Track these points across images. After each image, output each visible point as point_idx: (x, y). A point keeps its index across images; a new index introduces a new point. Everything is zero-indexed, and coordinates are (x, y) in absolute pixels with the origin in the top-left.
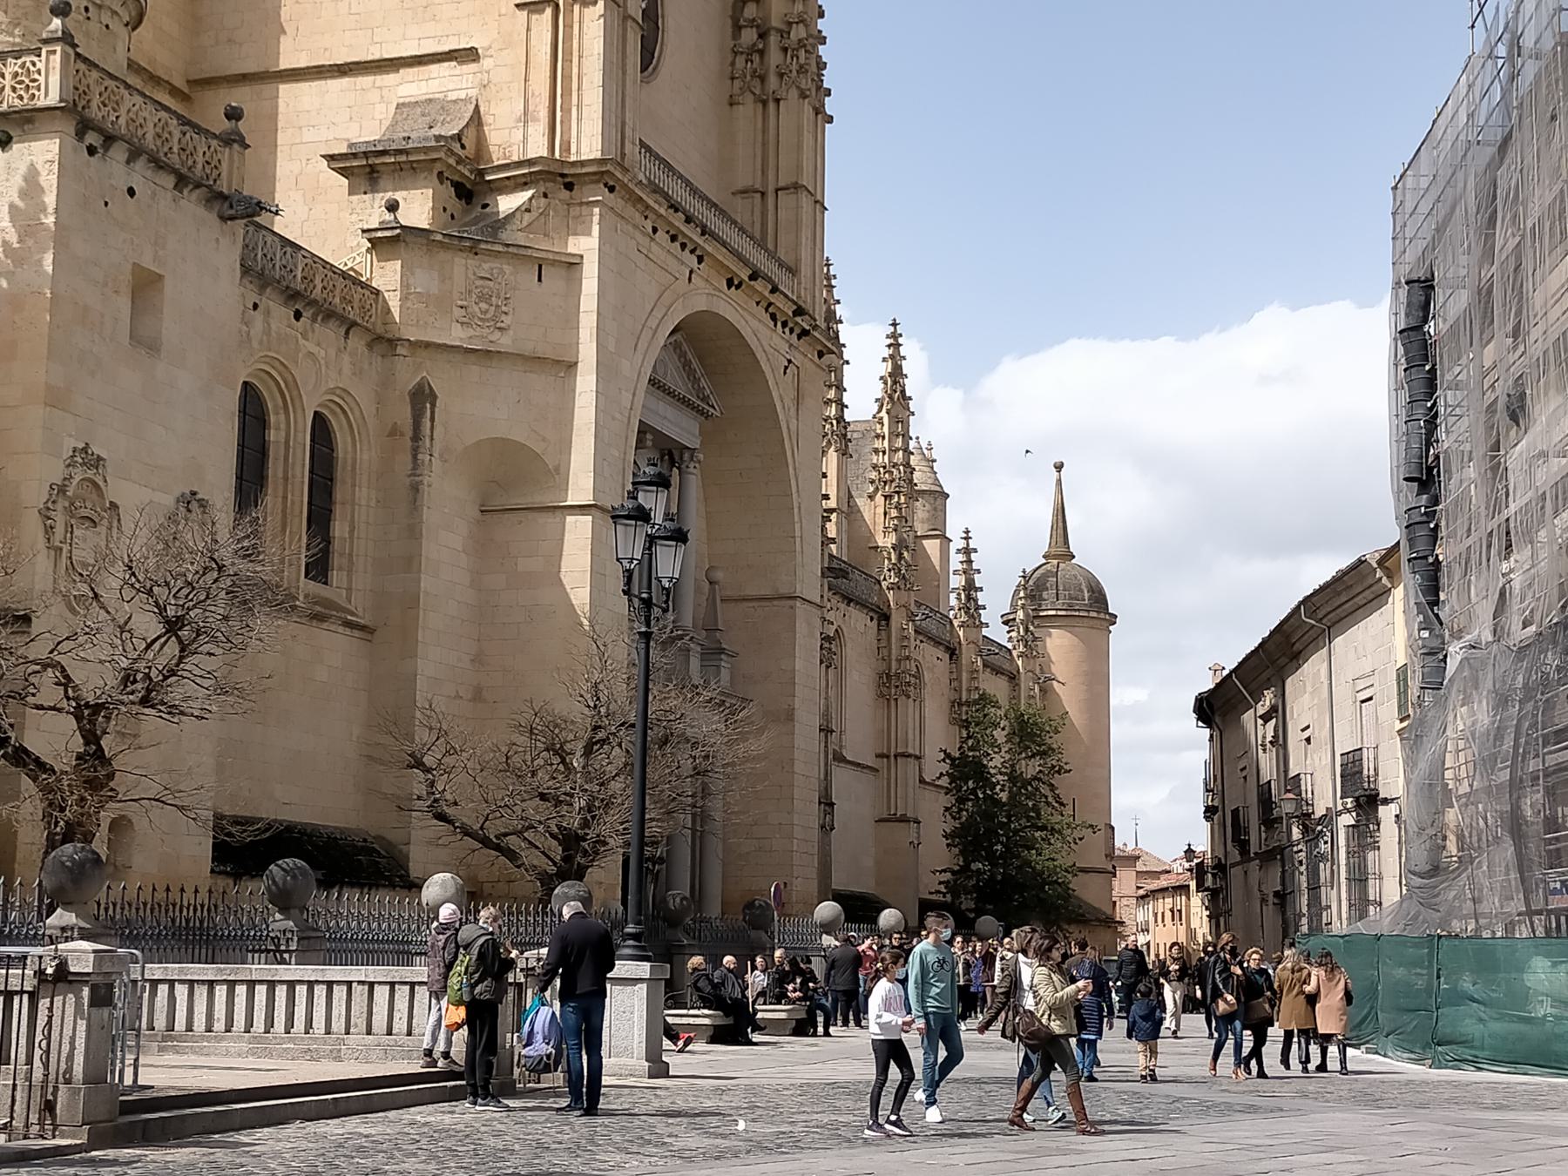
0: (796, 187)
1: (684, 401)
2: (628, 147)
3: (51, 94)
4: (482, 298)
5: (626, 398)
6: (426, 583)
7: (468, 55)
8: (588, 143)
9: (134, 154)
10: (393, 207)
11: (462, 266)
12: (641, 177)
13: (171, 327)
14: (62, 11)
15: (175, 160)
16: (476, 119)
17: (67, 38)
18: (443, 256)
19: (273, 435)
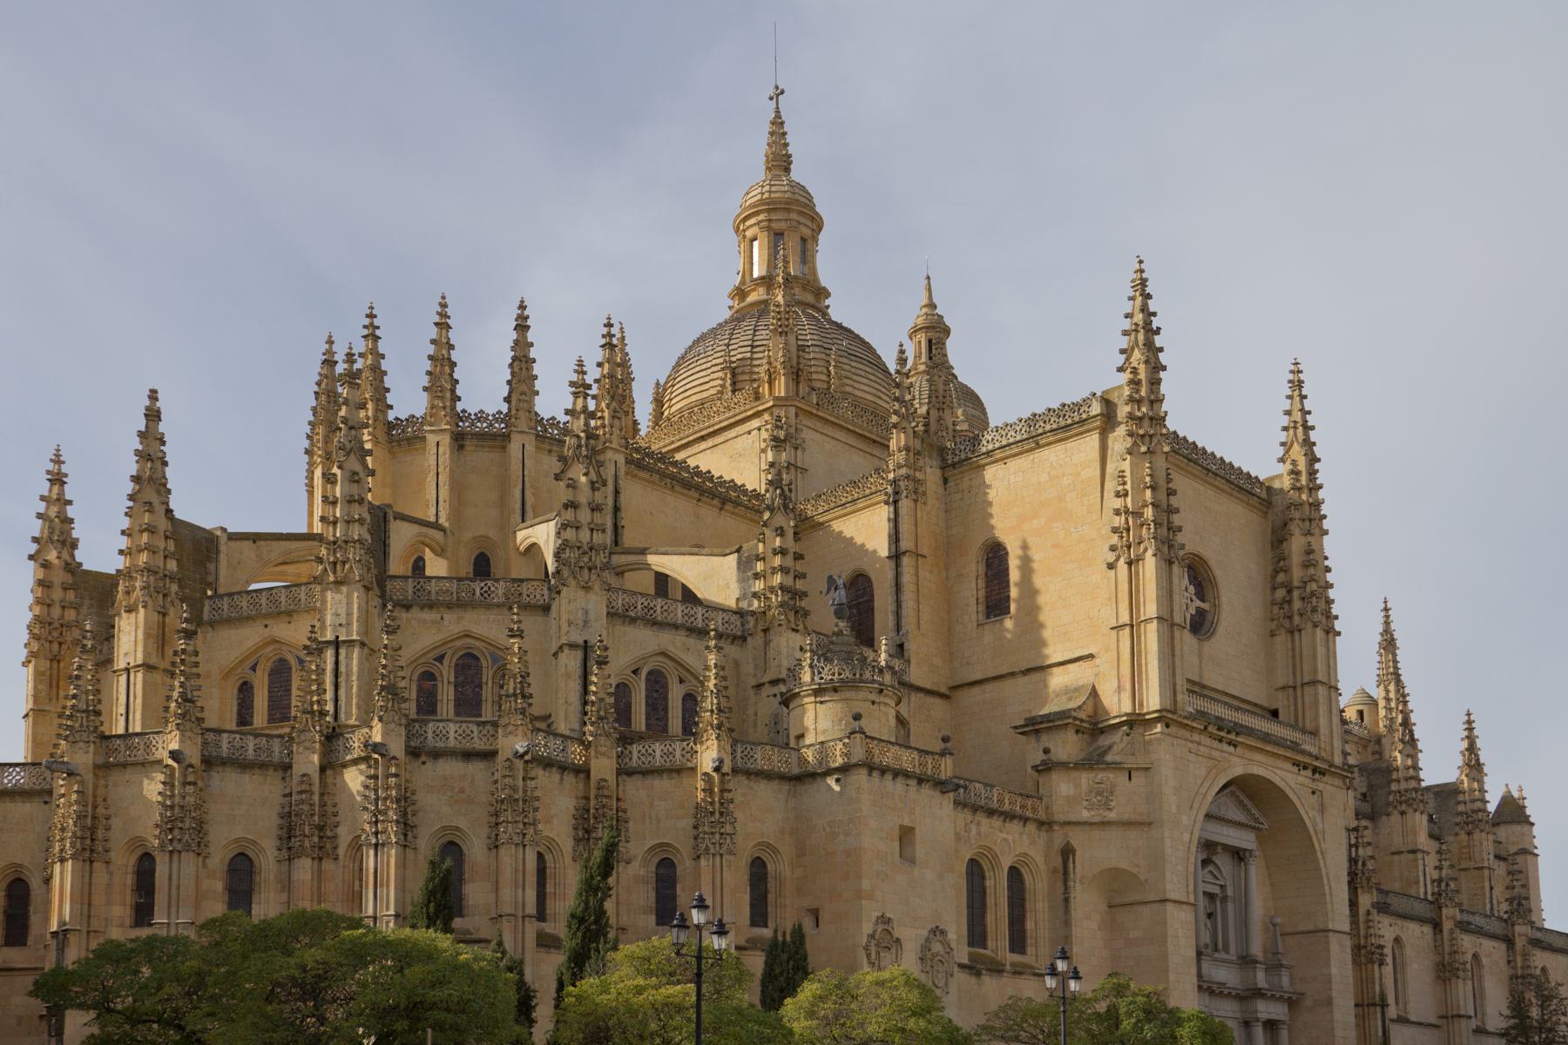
9: (896, 773)
13: (920, 851)
14: (857, 717)
15: (918, 771)
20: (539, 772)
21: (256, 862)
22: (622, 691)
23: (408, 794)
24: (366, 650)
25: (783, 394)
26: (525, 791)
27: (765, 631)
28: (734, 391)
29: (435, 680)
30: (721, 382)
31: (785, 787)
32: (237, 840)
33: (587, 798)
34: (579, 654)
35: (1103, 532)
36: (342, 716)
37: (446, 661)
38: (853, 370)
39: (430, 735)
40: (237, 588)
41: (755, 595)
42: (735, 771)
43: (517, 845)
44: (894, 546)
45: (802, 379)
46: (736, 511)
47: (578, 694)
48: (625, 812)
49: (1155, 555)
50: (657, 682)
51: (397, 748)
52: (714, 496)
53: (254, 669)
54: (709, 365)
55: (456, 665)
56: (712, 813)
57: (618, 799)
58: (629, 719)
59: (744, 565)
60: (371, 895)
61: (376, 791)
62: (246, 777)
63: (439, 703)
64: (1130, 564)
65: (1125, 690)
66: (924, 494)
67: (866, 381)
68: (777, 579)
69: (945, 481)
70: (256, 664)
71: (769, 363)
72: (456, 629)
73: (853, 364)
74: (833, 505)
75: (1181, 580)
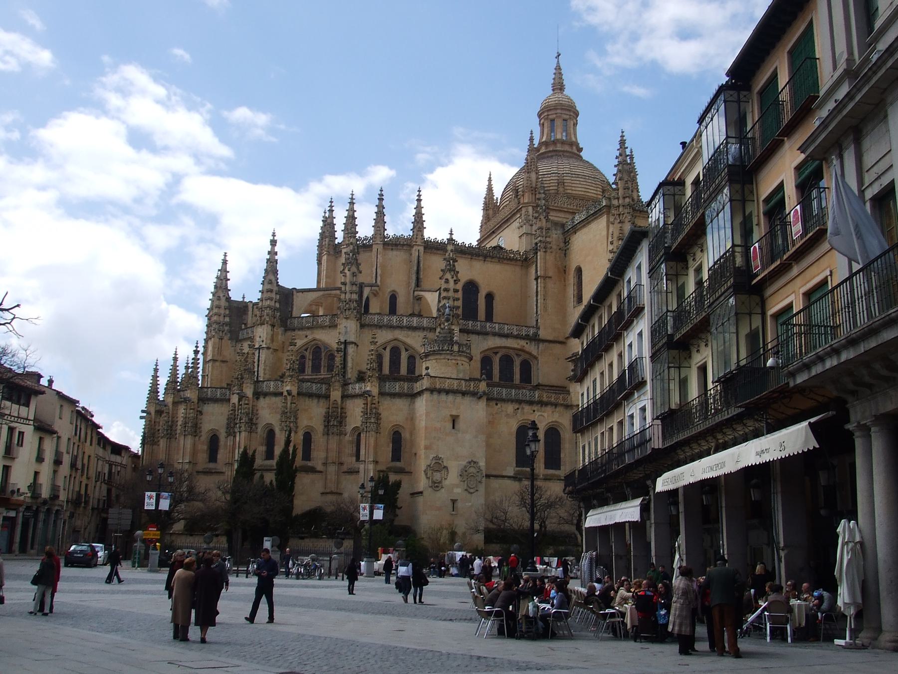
9: (448, 392)
13: (461, 424)
24: (271, 350)
25: (526, 201)
29: (305, 358)
31: (409, 399)
32: (212, 430)
33: (329, 408)
37: (308, 351)
38: (573, 182)
39: (265, 386)
40: (298, 316)
42: (382, 394)
45: (537, 192)
46: (493, 260)
48: (345, 413)
50: (395, 353)
52: (479, 256)
56: (367, 414)
57: (342, 408)
67: (580, 186)
72: (310, 337)
73: (572, 179)
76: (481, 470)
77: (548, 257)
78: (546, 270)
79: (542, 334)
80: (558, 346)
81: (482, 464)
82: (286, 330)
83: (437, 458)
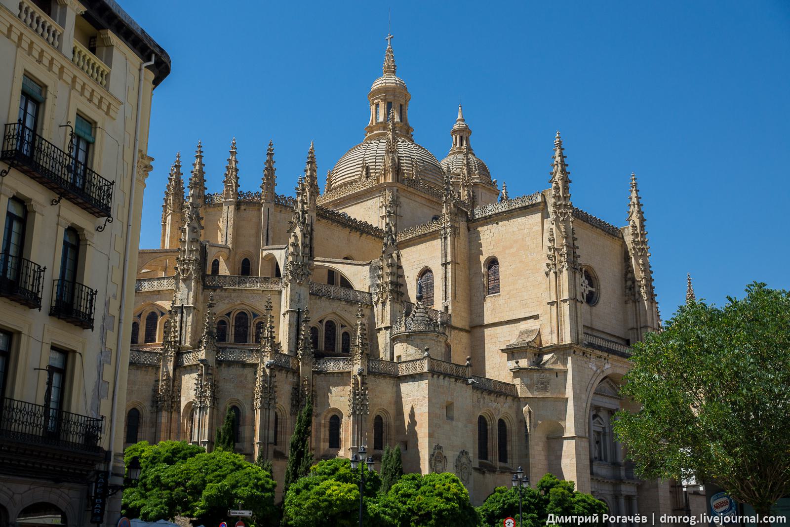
0: (646, 327)
1: (611, 397)
2: (580, 337)
3: (426, 370)
4: (542, 383)
5: (584, 405)
6: (531, 460)
7: (536, 317)
8: (567, 339)
10: (517, 363)
11: (535, 376)
12: (586, 342)
13: (456, 413)
14: (427, 350)
15: (455, 374)
16: (539, 334)
17: (429, 356)
18: (531, 374)
19: (488, 427)
20: (277, 373)
21: (141, 413)
22: (314, 330)
23: (216, 383)
25: (391, 181)
26: (271, 383)
27: (384, 303)
28: (367, 177)
29: (226, 324)
30: (360, 173)
34: (296, 315)
35: (543, 257)
36: (183, 342)
37: (231, 316)
41: (378, 285)
42: (369, 373)
43: (266, 409)
44: (444, 259)
47: (294, 334)
48: (316, 392)
49: (567, 270)
50: (330, 326)
51: (212, 362)
53: (139, 316)
54: (355, 164)
55: (236, 317)
57: (313, 386)
58: (317, 344)
59: (373, 270)
60: (196, 431)
61: (201, 381)
62: (139, 372)
63: (227, 336)
64: (556, 273)
65: (554, 333)
66: (459, 233)
68: (388, 280)
69: (469, 230)
70: (140, 314)
71: (385, 165)
74: (414, 235)
75: (581, 280)
76: (470, 461)
77: (456, 243)
78: (454, 255)
79: (455, 322)
80: (464, 334)
81: (471, 455)
82: (203, 289)
83: (439, 447)
